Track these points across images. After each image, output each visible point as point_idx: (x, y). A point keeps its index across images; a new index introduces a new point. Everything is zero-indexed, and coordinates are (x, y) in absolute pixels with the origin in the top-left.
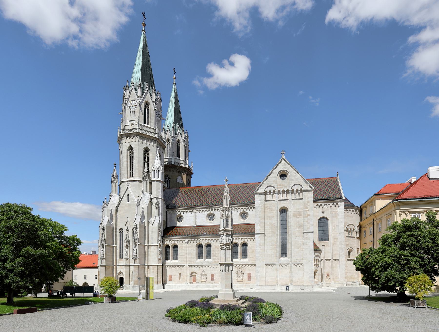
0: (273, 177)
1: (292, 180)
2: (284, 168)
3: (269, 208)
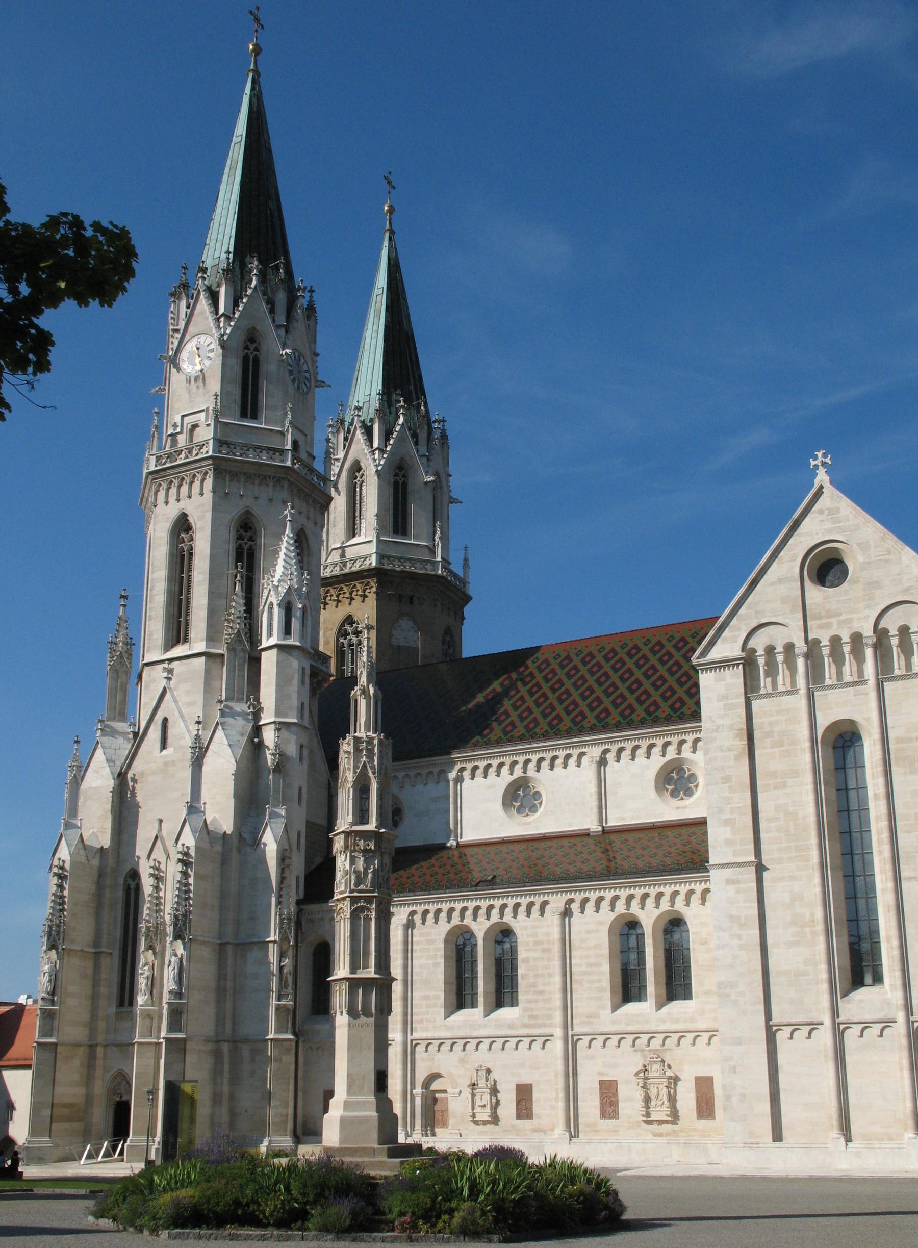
0: (780, 581)
1: (875, 584)
2: (829, 531)
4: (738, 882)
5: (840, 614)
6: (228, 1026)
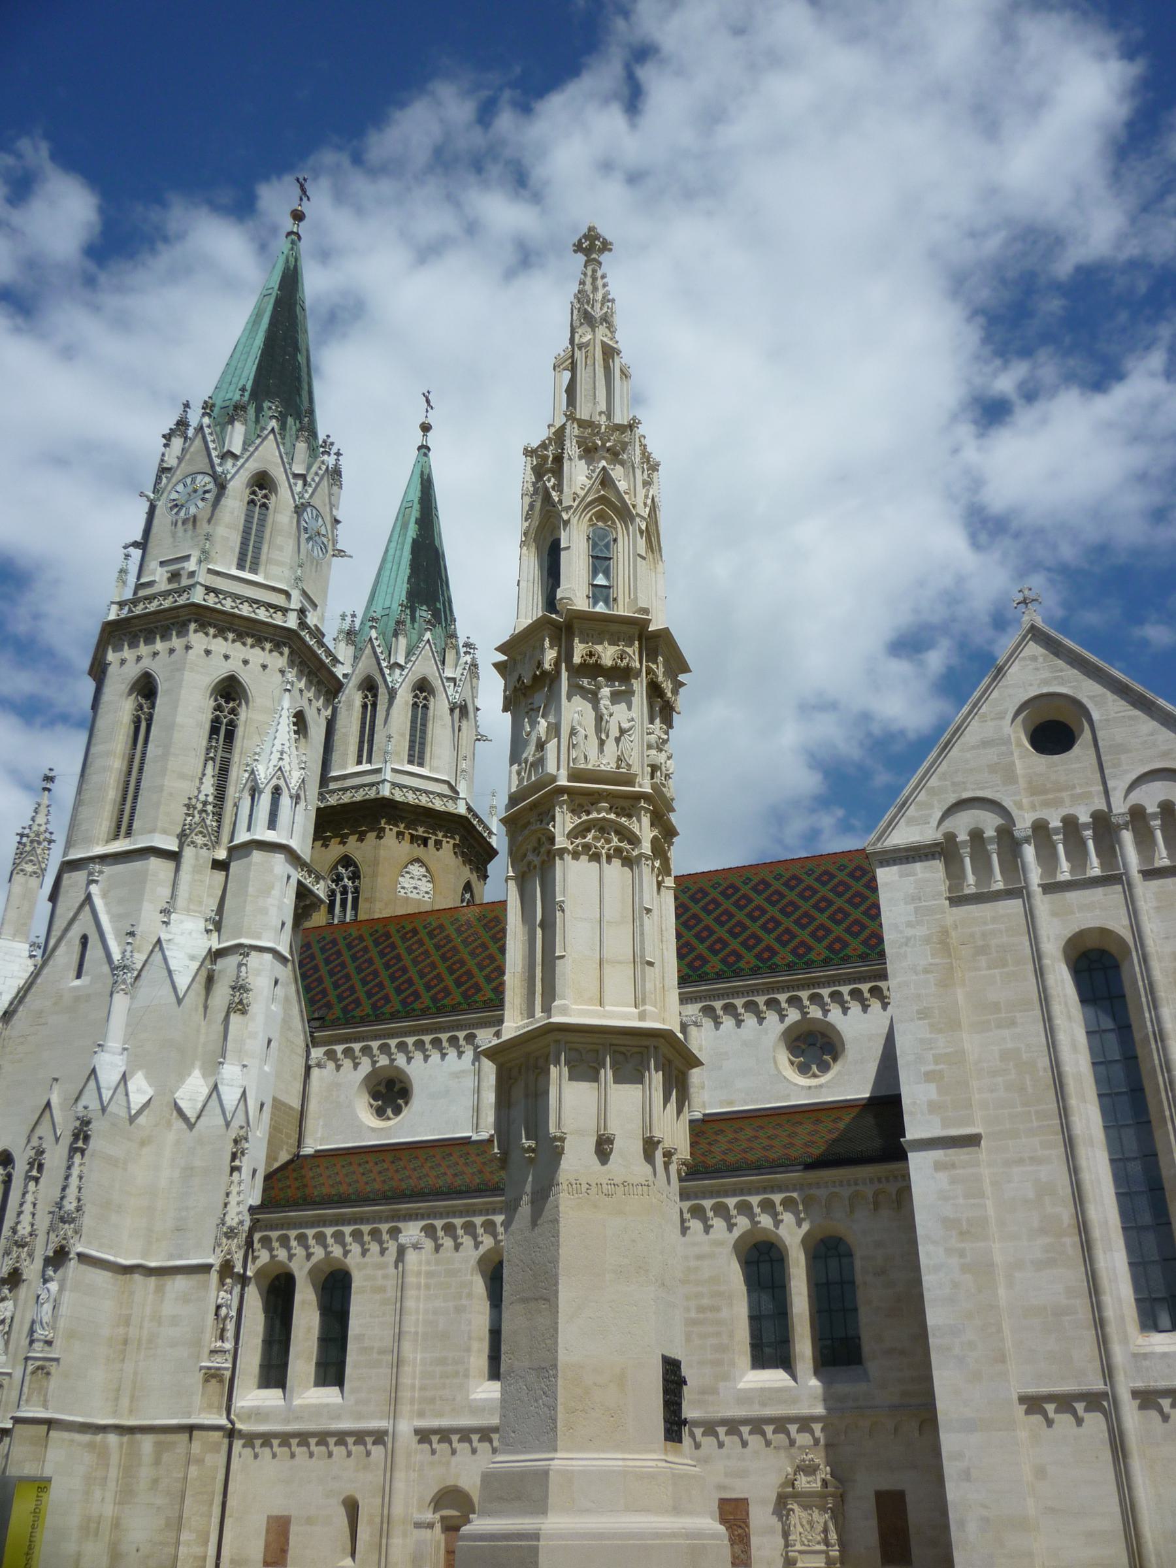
2: (1046, 682)
3: (982, 950)
4: (953, 1166)
5: (1074, 787)
6: (125, 1402)
